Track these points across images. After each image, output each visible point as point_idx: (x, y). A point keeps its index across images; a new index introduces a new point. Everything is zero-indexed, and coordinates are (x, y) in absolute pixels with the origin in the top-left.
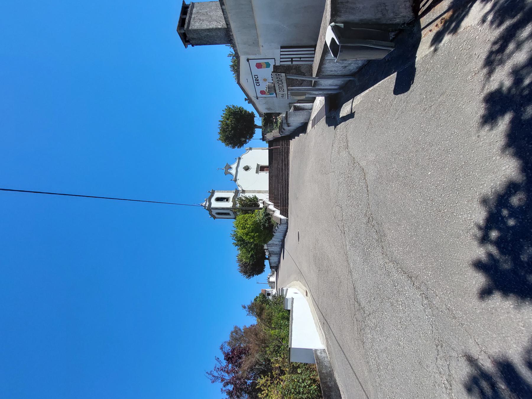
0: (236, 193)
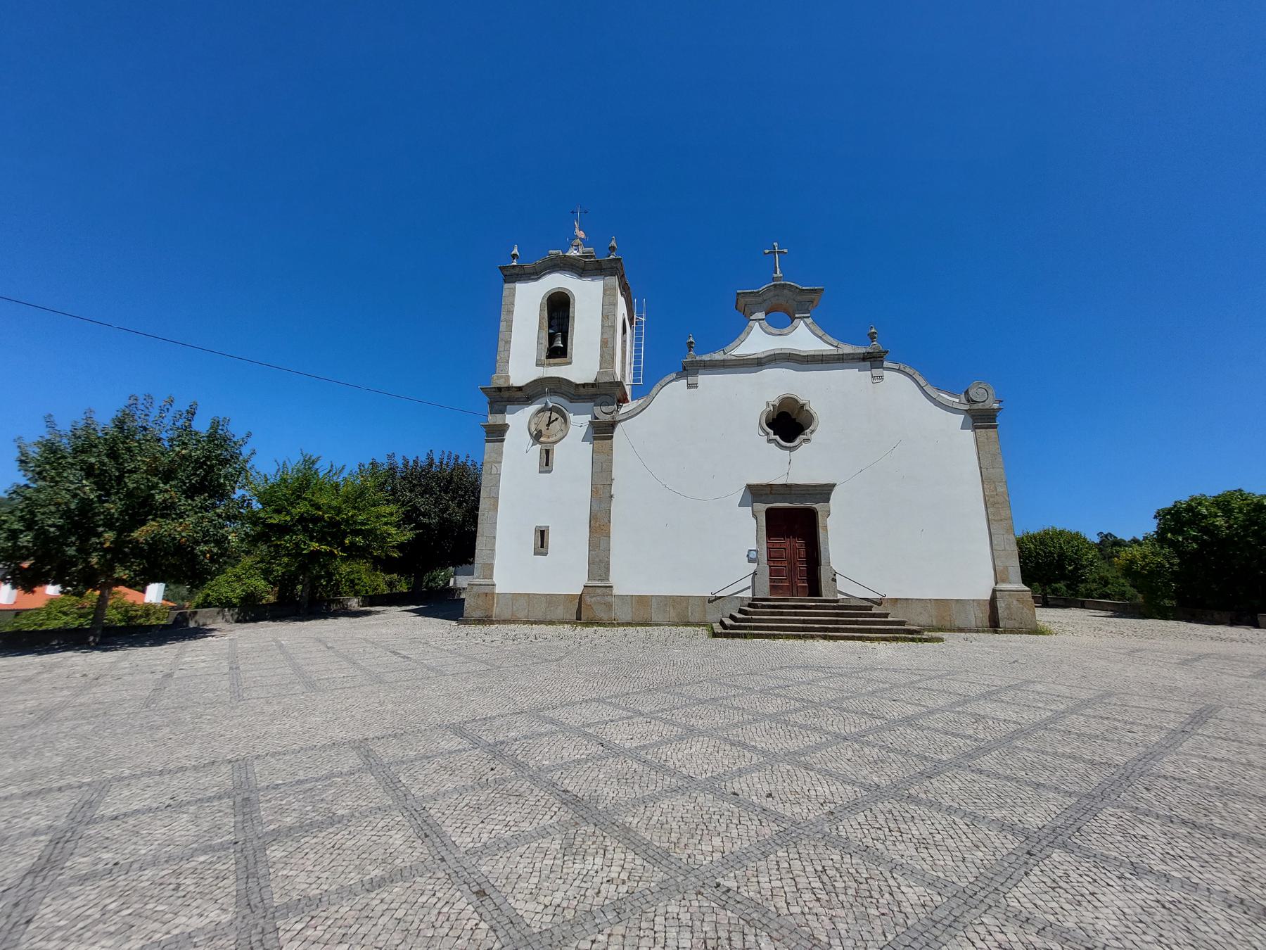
0: (592, 390)
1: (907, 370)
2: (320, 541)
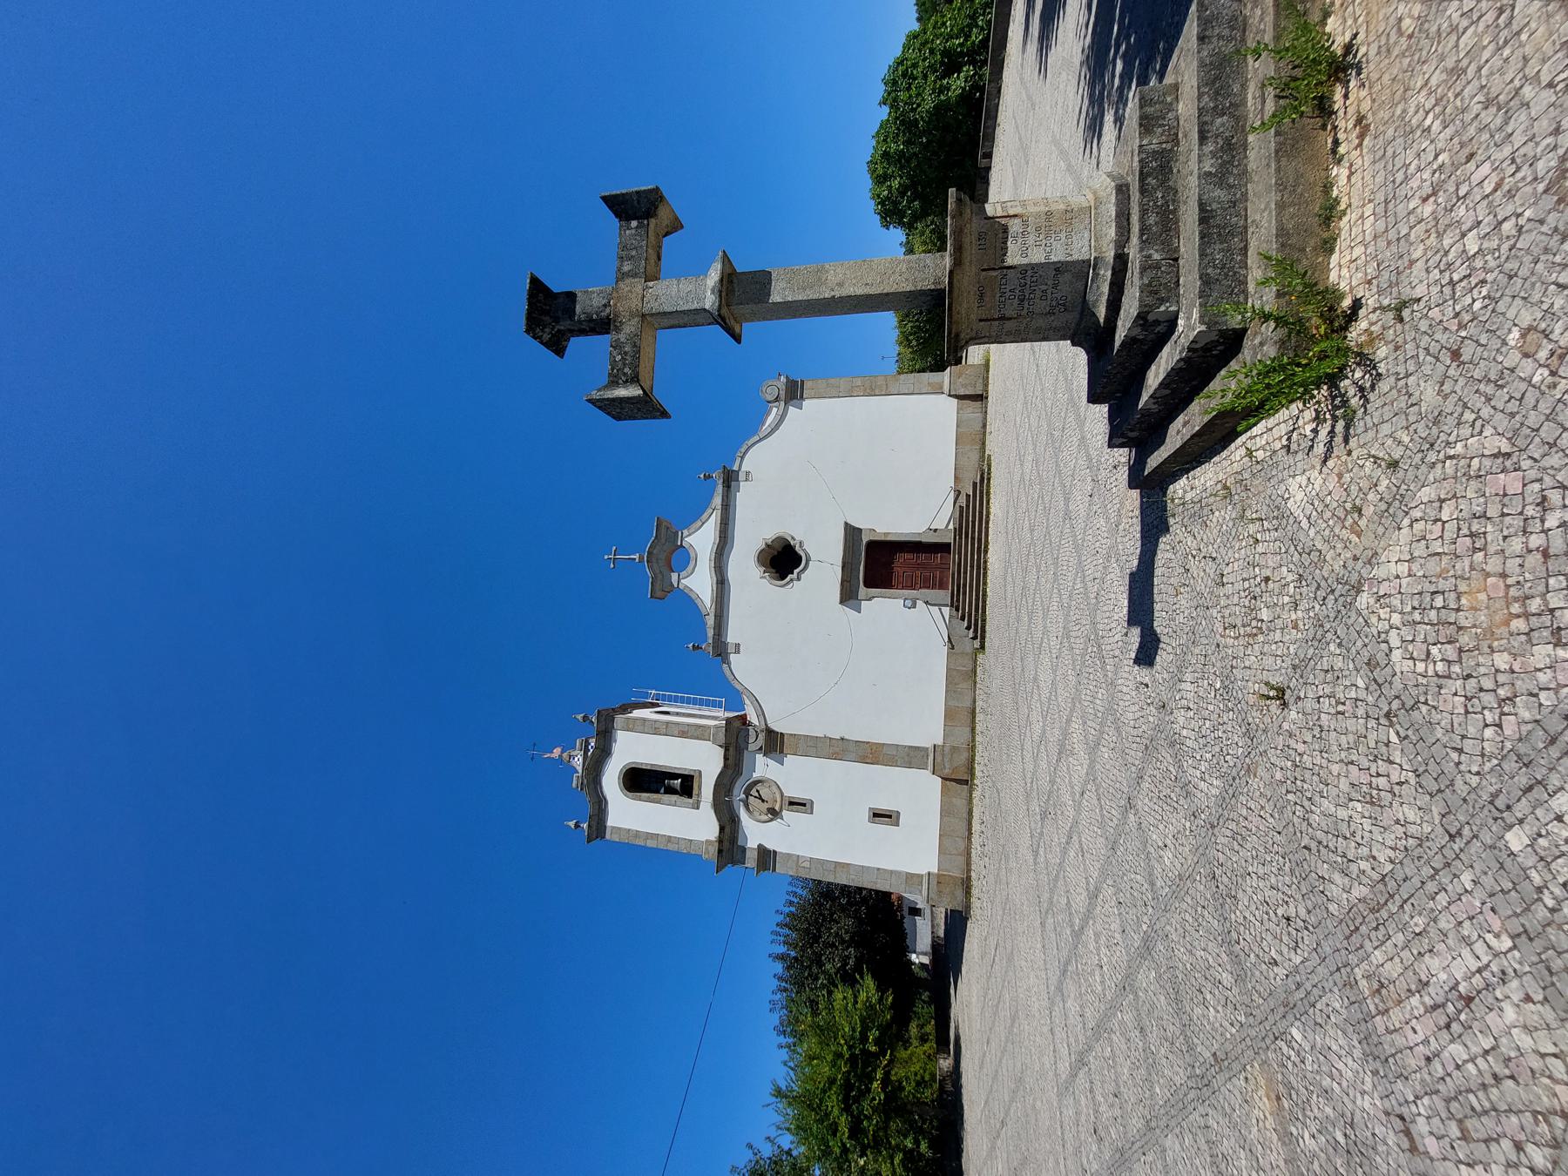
1: (743, 450)
2: (872, 1080)
